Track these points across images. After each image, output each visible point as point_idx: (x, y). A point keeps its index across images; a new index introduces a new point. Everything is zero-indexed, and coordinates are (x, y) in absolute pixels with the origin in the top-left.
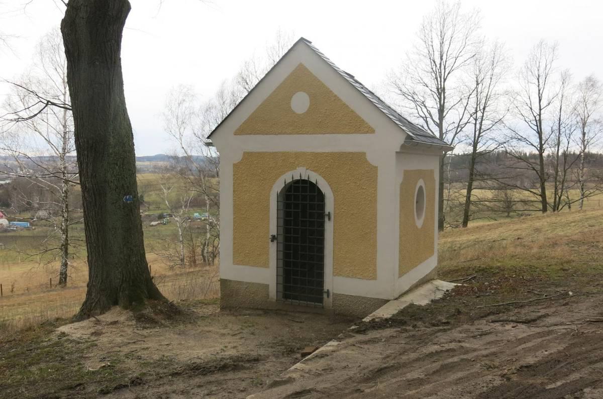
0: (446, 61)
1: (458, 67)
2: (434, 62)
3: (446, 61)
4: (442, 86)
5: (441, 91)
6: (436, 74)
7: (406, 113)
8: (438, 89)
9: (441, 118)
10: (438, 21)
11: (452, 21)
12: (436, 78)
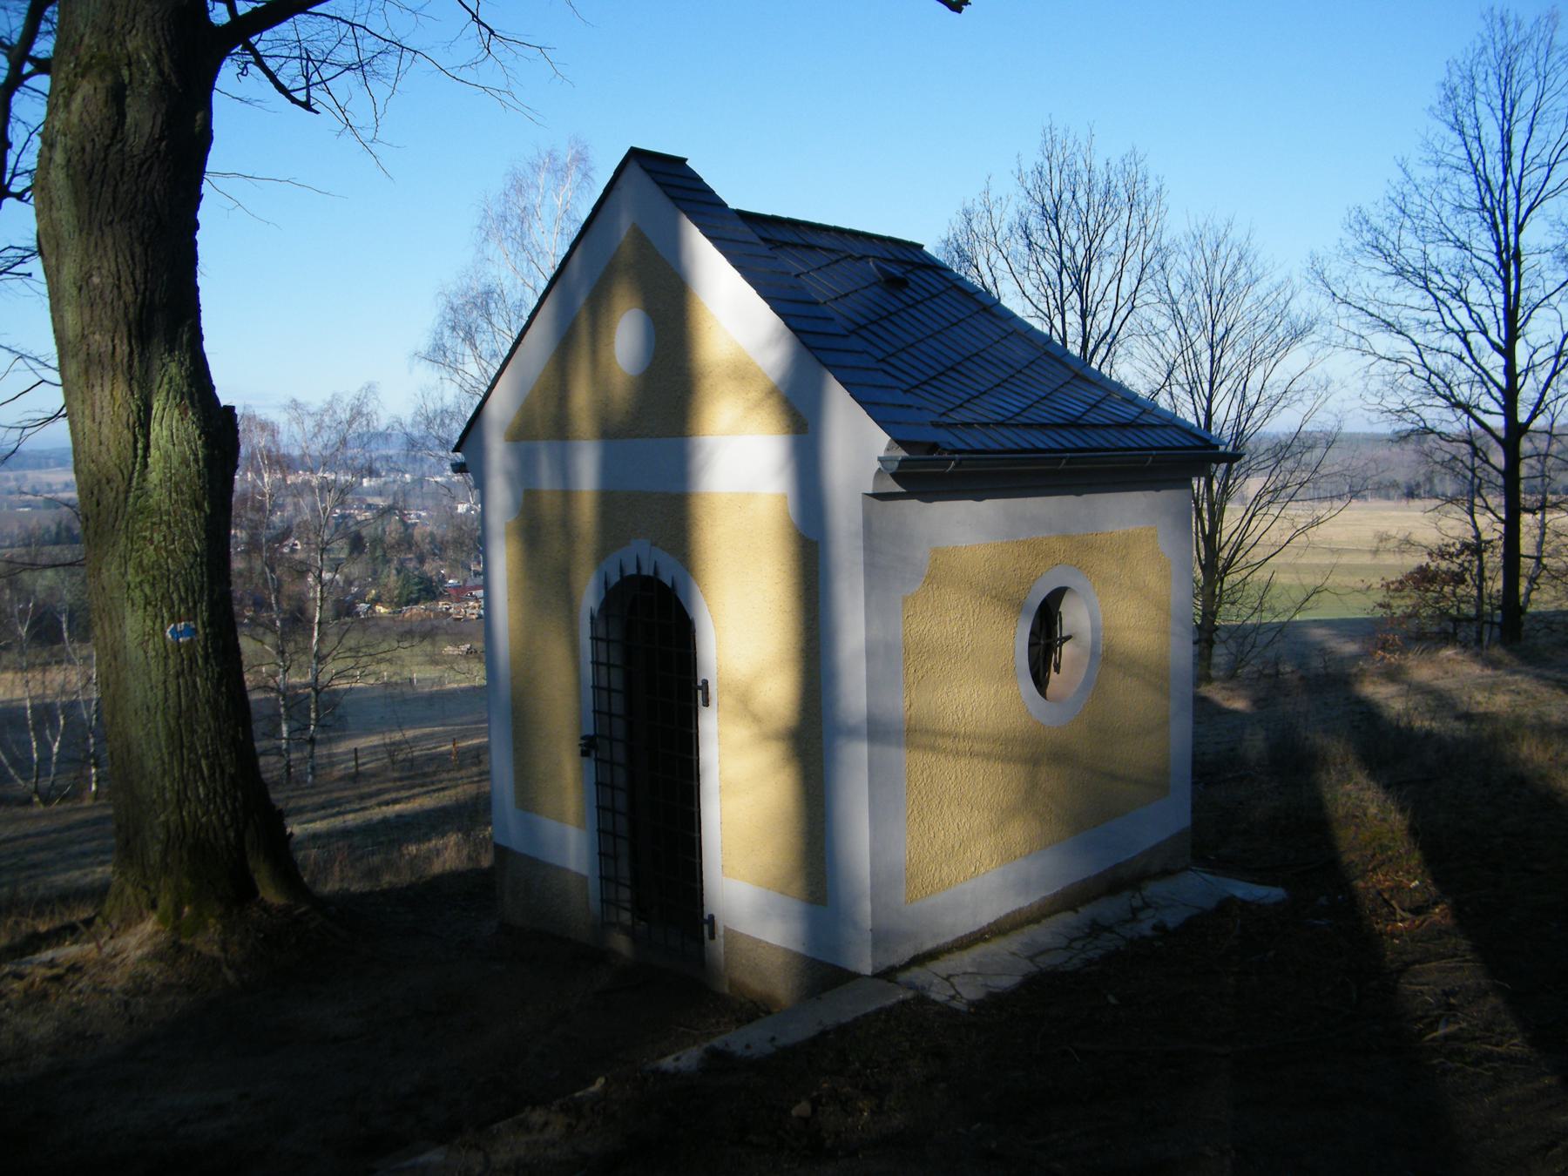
0: (1521, 177)
1: (1556, 192)
2: (1487, 182)
3: (1521, 177)
4: (1512, 243)
5: (1509, 259)
6: (1492, 215)
7: (1413, 323)
8: (1499, 254)
9: (1512, 334)
10: (1490, 71)
11: (1536, 66)
12: (1494, 226)
